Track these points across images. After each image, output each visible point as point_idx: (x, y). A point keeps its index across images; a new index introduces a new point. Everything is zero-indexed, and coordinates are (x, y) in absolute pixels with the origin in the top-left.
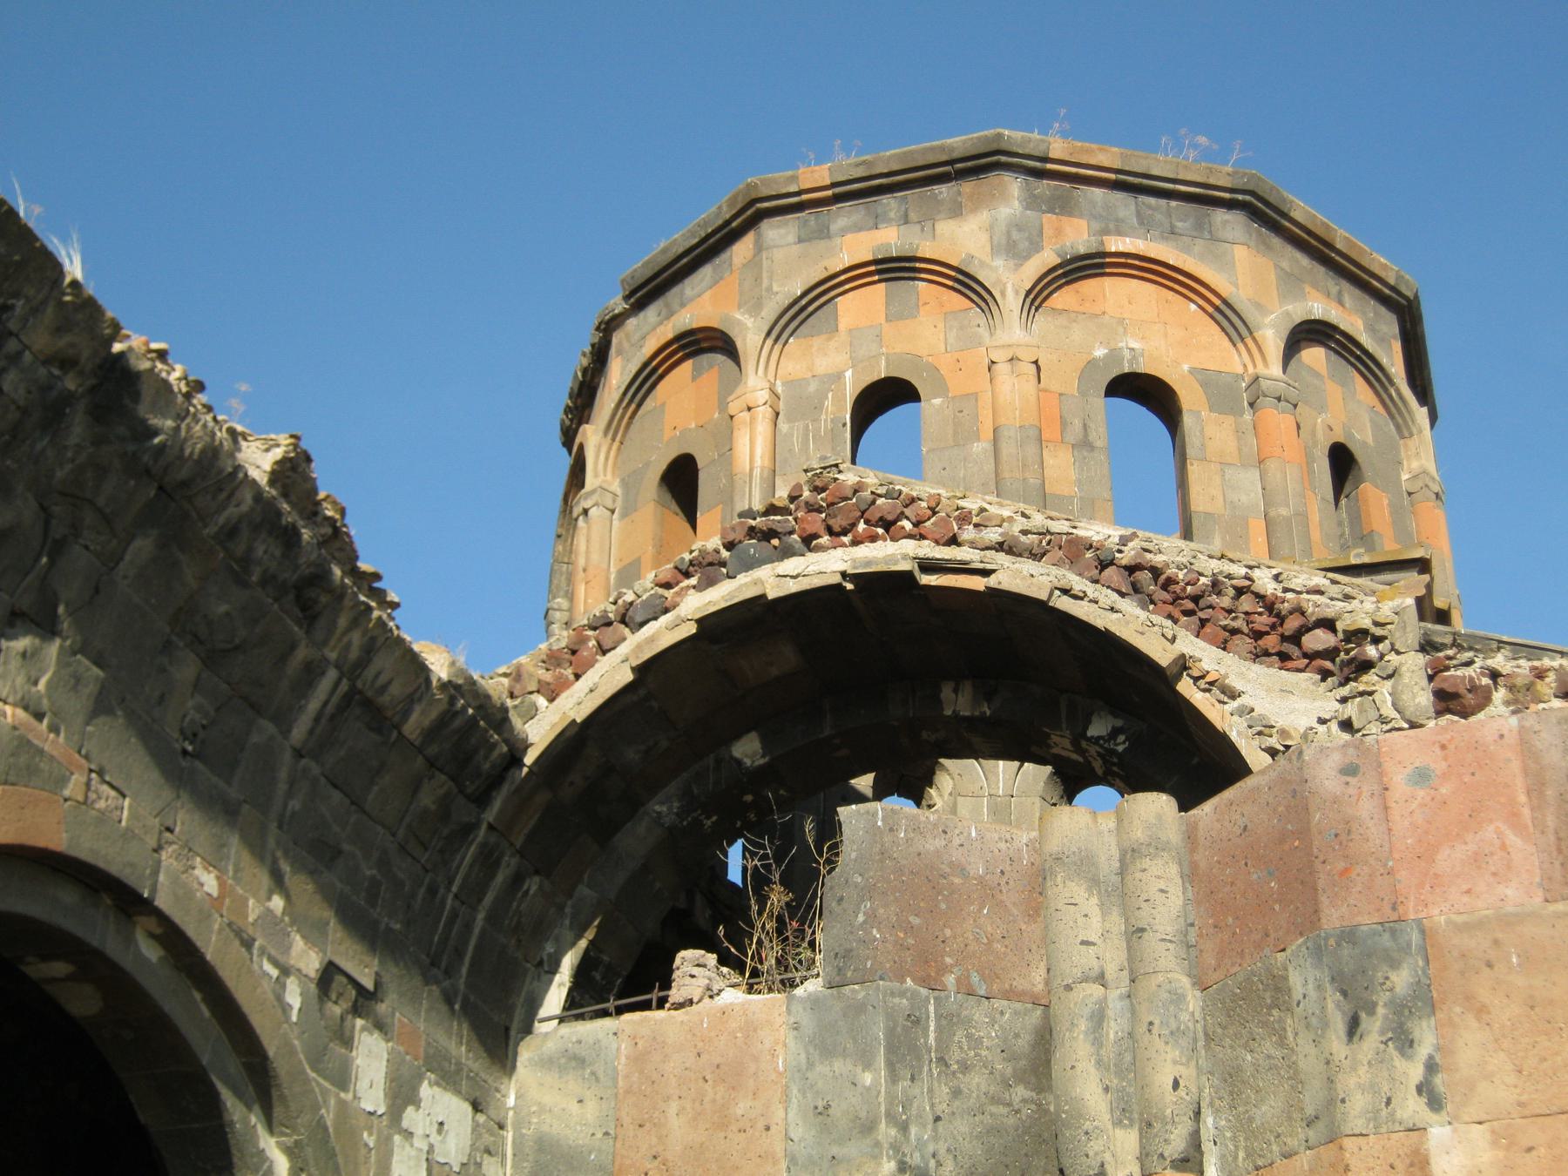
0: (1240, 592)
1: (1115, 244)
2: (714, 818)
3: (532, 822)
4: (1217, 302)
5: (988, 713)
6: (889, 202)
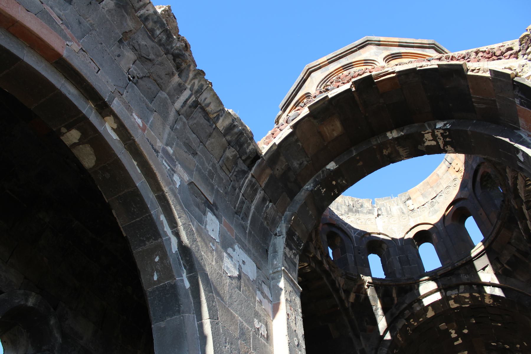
2: (325, 190)
3: (266, 180)
5: (403, 134)
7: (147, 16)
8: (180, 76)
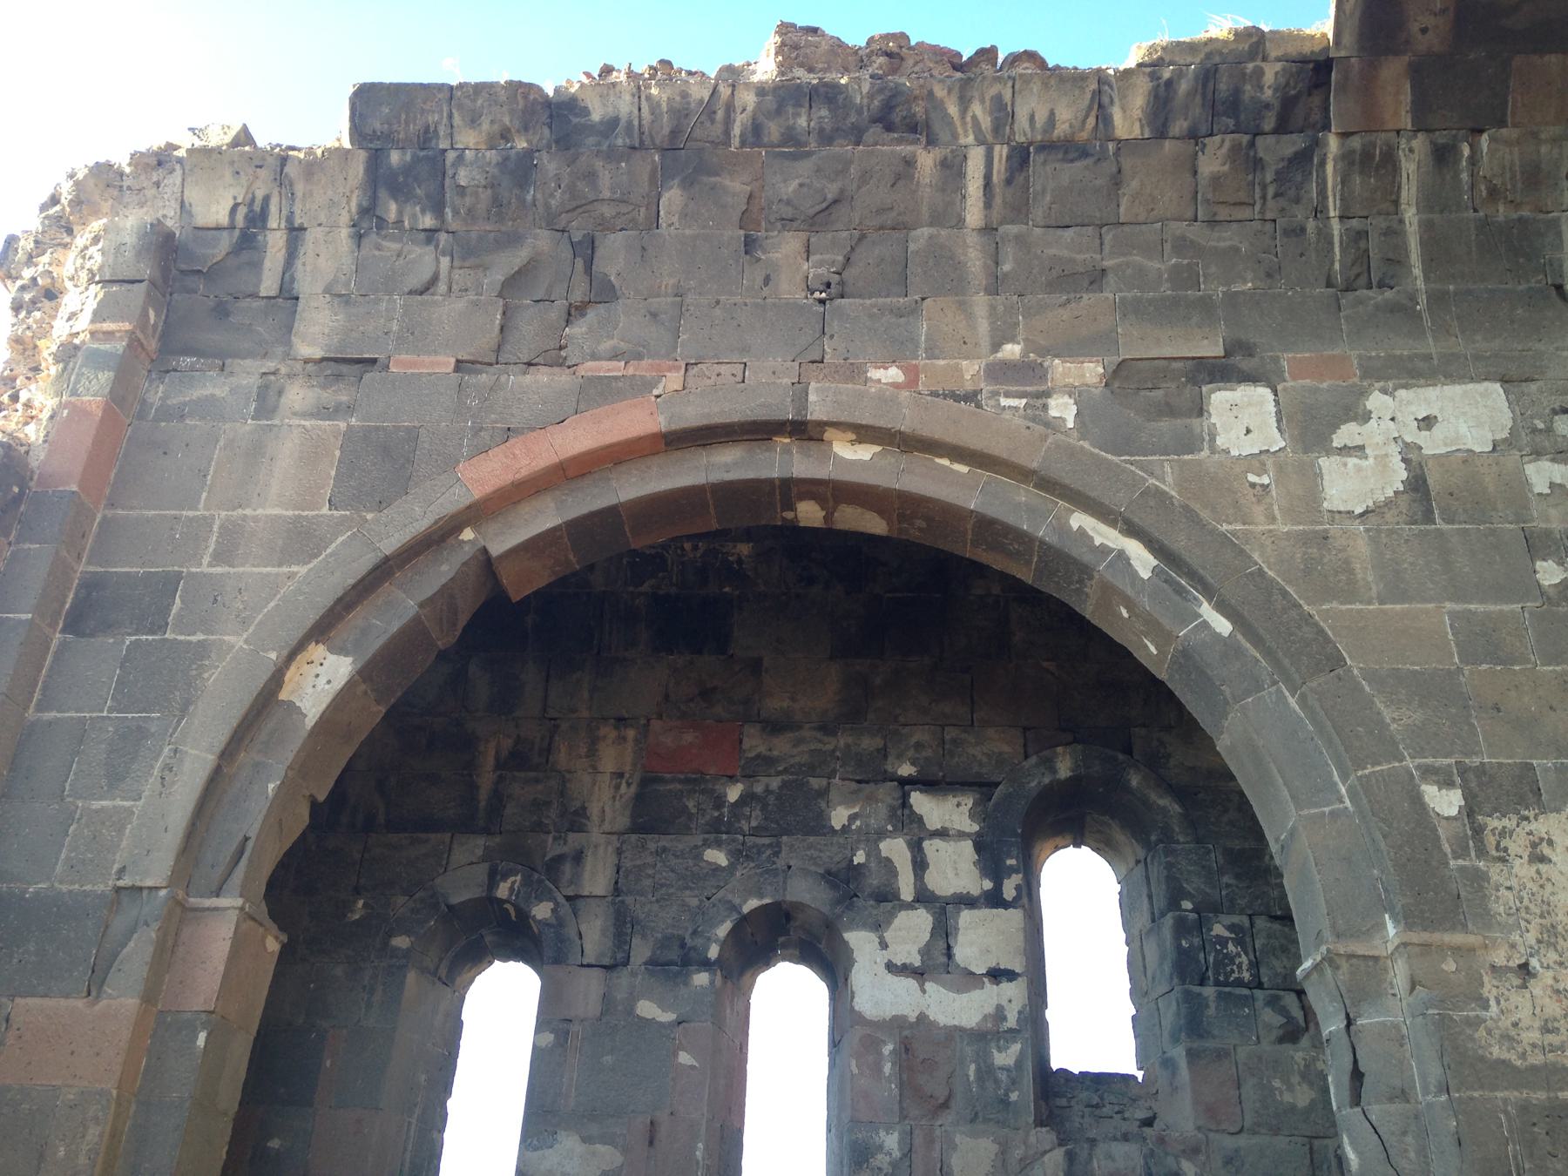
3: (1407, 97)
7: (753, 123)
8: (931, 142)
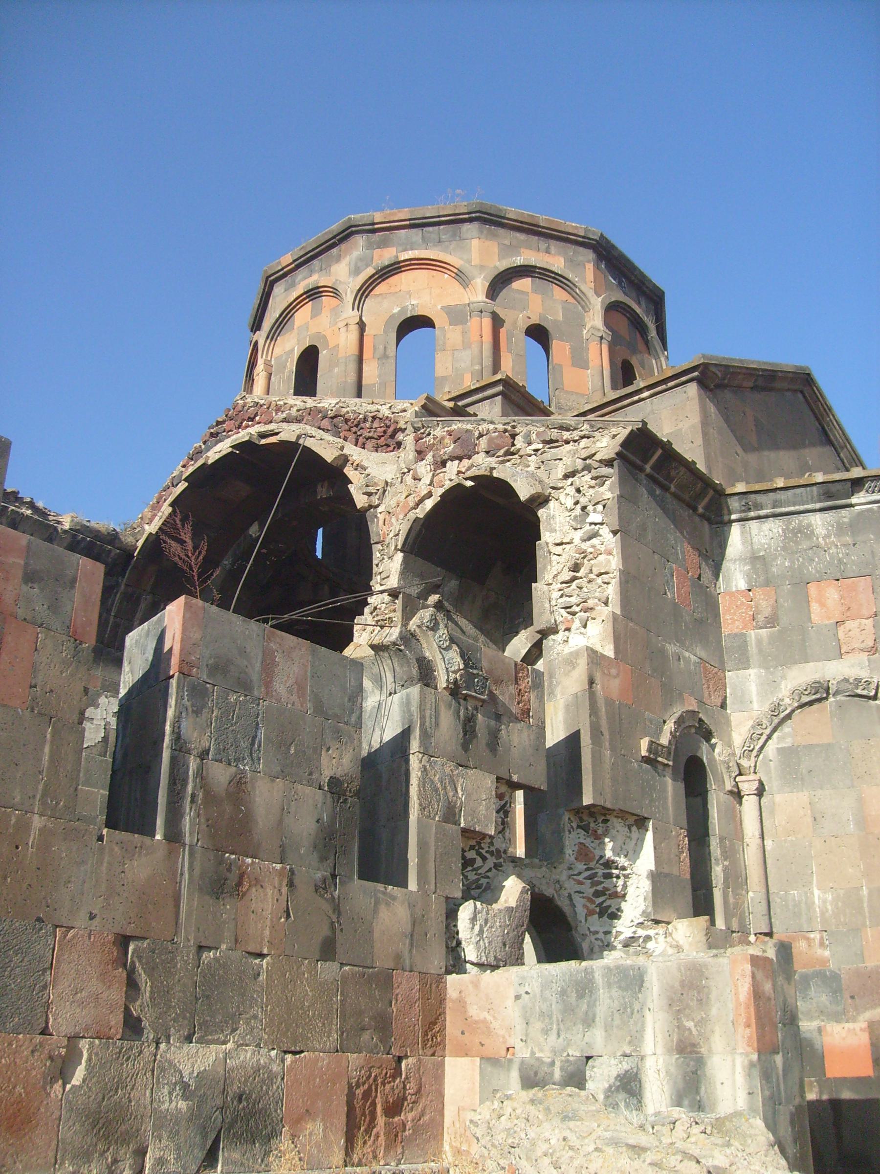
0: (374, 418)
1: (404, 256)
4: (456, 271)
6: (316, 263)
